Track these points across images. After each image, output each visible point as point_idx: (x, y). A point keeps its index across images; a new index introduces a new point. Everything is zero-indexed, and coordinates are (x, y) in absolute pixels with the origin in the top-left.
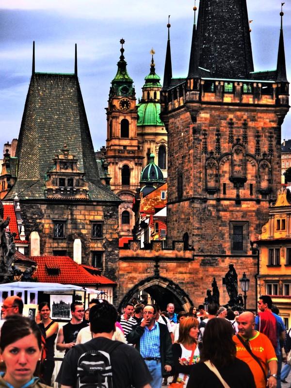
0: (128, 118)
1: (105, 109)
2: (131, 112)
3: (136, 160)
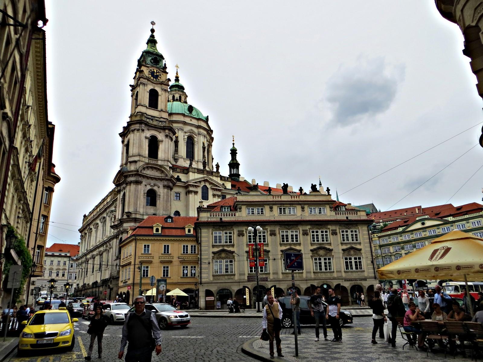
0: (158, 89)
1: (130, 85)
2: (162, 83)
3: (167, 131)
